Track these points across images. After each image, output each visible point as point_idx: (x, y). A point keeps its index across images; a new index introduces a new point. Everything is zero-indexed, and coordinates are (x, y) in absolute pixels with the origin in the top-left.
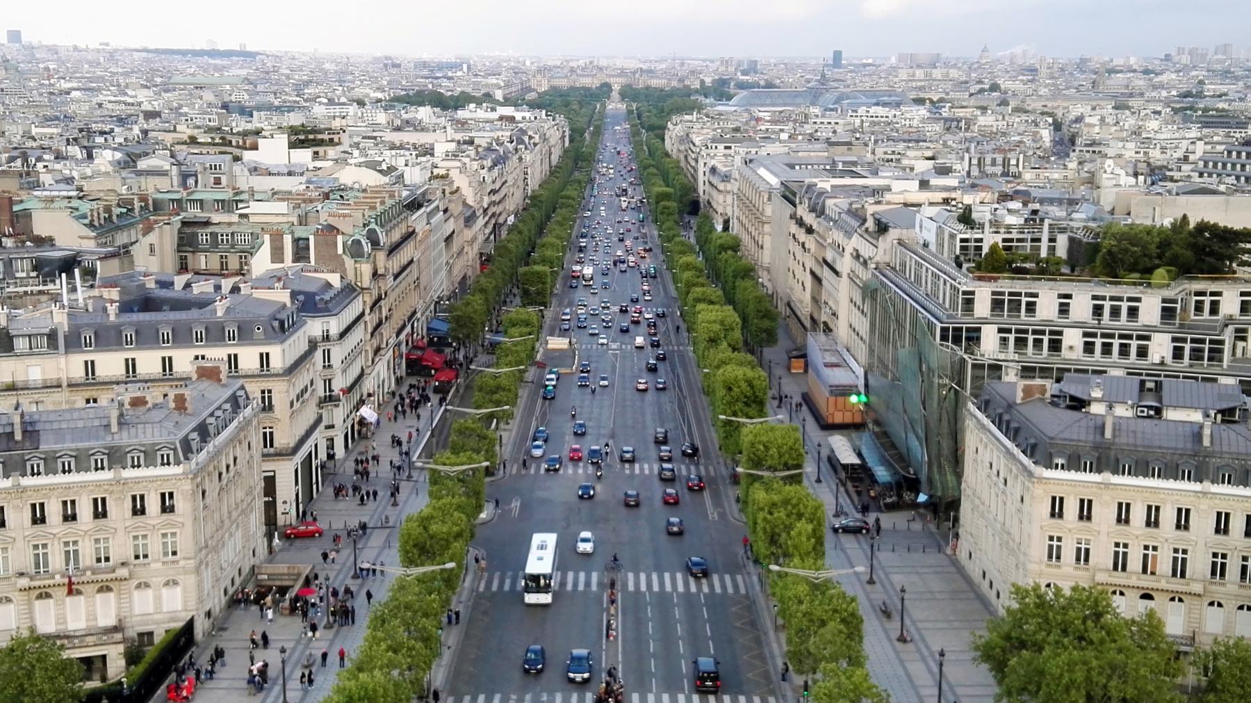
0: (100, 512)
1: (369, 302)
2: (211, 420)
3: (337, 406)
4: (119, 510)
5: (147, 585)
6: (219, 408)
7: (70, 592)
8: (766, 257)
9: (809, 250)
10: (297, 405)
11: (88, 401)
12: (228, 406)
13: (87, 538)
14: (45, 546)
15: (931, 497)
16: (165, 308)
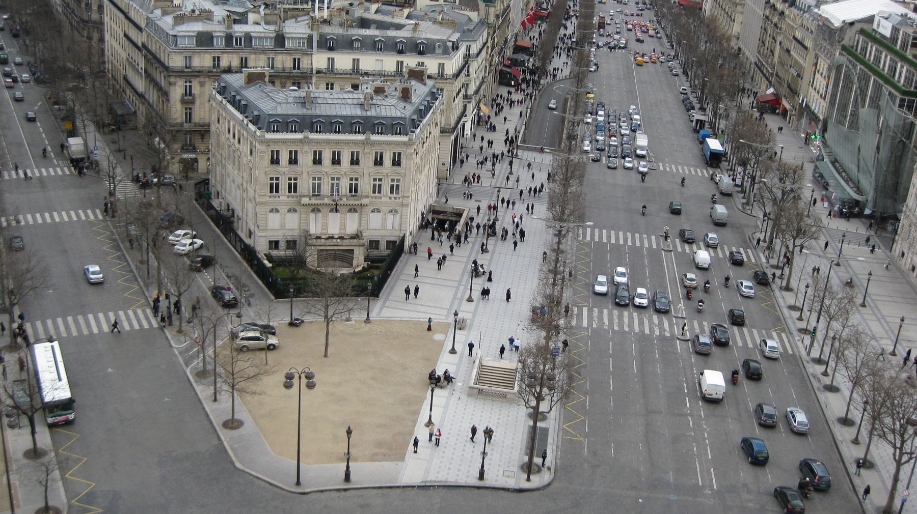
0: (355, 162)
1: (491, 33)
2: (423, 108)
3: (469, 102)
4: (367, 161)
5: (379, 211)
6: (424, 100)
7: (331, 211)
8: (736, 29)
9: (781, 28)
10: (457, 100)
11: (327, 85)
12: (429, 99)
13: (345, 177)
14: (320, 179)
15: (873, 212)
16: (373, 26)
